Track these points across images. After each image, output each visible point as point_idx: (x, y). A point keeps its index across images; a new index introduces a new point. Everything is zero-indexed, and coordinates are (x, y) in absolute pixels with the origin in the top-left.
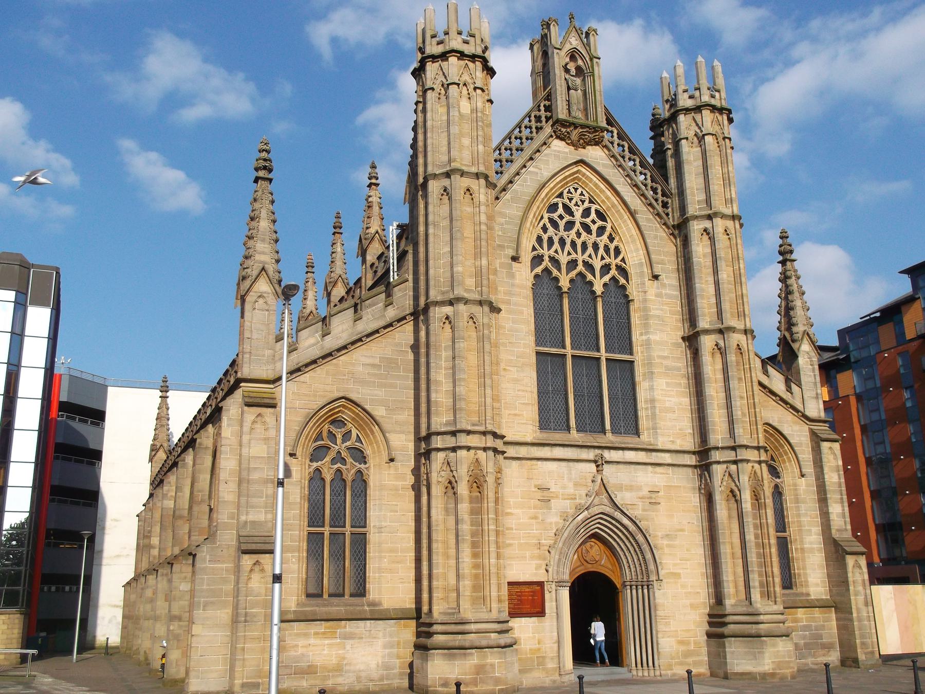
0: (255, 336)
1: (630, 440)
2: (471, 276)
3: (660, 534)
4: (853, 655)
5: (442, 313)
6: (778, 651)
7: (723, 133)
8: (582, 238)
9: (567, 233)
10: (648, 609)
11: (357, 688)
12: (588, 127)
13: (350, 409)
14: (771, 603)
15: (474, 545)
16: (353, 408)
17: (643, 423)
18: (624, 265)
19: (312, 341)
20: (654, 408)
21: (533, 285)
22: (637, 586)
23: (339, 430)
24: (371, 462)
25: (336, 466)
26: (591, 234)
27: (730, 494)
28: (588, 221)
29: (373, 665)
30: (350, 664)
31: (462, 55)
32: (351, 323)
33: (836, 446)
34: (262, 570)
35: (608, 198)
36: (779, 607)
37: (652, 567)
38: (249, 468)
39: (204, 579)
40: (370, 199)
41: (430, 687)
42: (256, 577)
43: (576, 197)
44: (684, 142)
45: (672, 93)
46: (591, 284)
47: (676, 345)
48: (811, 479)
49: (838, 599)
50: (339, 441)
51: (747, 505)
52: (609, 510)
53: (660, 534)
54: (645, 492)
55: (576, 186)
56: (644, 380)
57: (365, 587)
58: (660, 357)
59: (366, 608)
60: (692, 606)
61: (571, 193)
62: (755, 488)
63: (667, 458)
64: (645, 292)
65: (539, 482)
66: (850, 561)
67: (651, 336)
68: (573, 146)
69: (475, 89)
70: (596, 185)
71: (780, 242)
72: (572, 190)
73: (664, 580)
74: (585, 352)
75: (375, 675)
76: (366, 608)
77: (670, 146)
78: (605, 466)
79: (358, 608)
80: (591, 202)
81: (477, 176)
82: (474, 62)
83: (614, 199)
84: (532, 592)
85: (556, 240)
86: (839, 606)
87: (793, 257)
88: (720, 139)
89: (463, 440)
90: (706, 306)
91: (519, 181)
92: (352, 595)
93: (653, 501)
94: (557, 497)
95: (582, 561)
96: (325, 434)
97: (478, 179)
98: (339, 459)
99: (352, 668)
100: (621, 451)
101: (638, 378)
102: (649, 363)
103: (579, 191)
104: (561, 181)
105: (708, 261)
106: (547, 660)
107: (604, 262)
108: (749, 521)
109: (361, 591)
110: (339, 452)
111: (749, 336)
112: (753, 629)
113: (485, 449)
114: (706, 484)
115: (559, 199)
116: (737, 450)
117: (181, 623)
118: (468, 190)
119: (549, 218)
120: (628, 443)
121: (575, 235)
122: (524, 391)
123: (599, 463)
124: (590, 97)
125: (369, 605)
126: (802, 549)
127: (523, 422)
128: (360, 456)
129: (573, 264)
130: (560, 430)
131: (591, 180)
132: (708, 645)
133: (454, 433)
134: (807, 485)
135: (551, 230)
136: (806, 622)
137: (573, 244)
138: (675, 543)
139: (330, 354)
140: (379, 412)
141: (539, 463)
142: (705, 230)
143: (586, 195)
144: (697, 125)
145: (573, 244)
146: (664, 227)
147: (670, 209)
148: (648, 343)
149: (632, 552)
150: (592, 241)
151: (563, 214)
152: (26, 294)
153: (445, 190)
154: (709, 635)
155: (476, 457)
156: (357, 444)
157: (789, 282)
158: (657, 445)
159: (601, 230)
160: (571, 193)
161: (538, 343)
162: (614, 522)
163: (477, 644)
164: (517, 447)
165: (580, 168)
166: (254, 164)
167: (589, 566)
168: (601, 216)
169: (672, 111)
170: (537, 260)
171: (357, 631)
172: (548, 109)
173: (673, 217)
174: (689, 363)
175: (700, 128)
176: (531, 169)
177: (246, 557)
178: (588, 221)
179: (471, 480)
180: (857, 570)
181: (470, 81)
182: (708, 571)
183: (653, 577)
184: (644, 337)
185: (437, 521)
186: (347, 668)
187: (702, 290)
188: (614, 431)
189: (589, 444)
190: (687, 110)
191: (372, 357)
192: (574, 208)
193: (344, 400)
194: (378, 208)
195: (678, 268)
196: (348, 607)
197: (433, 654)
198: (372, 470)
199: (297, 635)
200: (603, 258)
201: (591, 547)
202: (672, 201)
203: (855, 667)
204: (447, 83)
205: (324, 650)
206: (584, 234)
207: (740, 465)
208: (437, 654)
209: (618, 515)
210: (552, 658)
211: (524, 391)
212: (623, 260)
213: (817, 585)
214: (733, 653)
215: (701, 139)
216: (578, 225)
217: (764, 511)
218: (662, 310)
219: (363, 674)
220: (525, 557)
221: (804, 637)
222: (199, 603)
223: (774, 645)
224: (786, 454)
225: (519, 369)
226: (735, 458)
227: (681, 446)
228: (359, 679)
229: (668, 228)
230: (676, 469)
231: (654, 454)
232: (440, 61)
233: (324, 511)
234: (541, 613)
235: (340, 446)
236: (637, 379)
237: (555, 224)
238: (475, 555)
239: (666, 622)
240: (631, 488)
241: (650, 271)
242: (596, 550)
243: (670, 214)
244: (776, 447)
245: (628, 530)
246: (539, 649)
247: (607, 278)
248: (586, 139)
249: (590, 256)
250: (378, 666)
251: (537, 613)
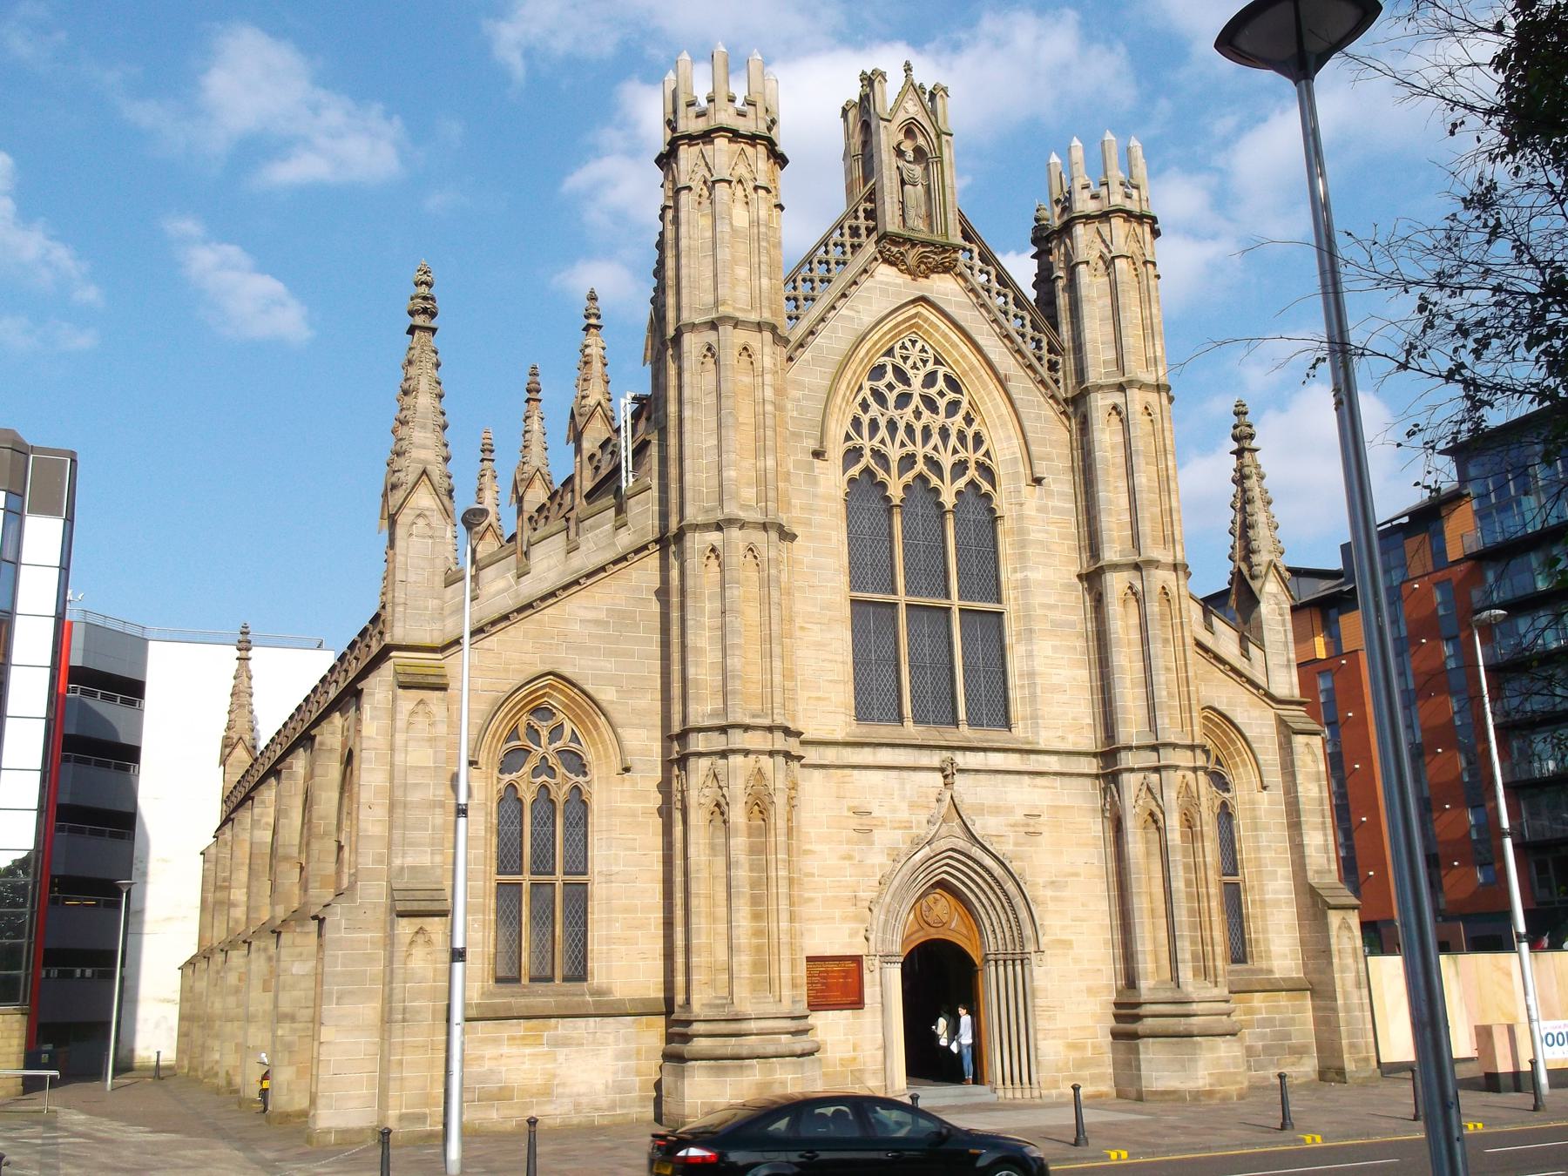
0: (412, 578)
1: (997, 736)
2: (749, 485)
3: (1041, 881)
4: (1336, 1064)
5: (704, 542)
6: (1219, 1058)
7: (1144, 254)
8: (924, 420)
9: (899, 411)
10: (1024, 995)
11: (575, 1121)
12: (933, 245)
13: (561, 691)
14: (1209, 985)
15: (755, 901)
16: (566, 689)
17: (1017, 709)
18: (989, 462)
19: (501, 584)
20: (1033, 685)
21: (847, 494)
22: (1005, 961)
23: (545, 724)
24: (595, 772)
25: (539, 780)
26: (937, 414)
27: (1150, 819)
28: (932, 392)
29: (600, 1087)
30: (564, 1085)
31: (735, 135)
32: (563, 554)
33: (1317, 741)
34: (429, 942)
35: (964, 356)
36: (1223, 991)
37: (1028, 931)
38: (406, 784)
39: (336, 956)
40: (588, 351)
41: (688, 1117)
42: (419, 952)
43: (914, 354)
44: (1082, 268)
45: (1066, 189)
46: (936, 491)
47: (1069, 587)
48: (1277, 793)
49: (1315, 977)
50: (544, 740)
51: (1175, 835)
52: (962, 844)
53: (1041, 881)
54: (1019, 817)
55: (914, 337)
56: (1018, 642)
57: (585, 966)
58: (1043, 606)
59: (589, 998)
60: (1090, 990)
61: (906, 349)
62: (1187, 809)
63: (1053, 763)
64: (1021, 505)
65: (855, 803)
66: (1334, 918)
67: (1029, 574)
68: (910, 274)
69: (756, 188)
70: (945, 336)
71: (1235, 420)
72: (908, 344)
73: (1048, 952)
74: (927, 600)
75: (603, 1101)
76: (589, 998)
77: (1061, 274)
78: (957, 777)
79: (576, 999)
80: (937, 362)
81: (759, 326)
82: (754, 146)
83: (974, 359)
84: (843, 971)
85: (882, 422)
86: (1317, 988)
87: (1254, 444)
88: (1139, 264)
89: (738, 739)
90: (1115, 526)
91: (824, 331)
92: (566, 979)
93: (1031, 830)
94: (882, 826)
95: (922, 923)
96: (522, 730)
97: (761, 331)
98: (544, 768)
99: (567, 1090)
100: (982, 754)
101: (1009, 639)
102: (1026, 616)
103: (919, 346)
104: (890, 330)
105: (1119, 457)
106: (867, 1076)
107: (957, 457)
108: (1177, 858)
109: (578, 972)
110: (544, 757)
111: (1181, 573)
112: (1181, 1025)
113: (771, 754)
114: (1113, 803)
115: (887, 358)
116: (1161, 751)
117: (295, 1025)
118: (745, 349)
119: (871, 389)
120: (993, 741)
121: (912, 416)
122: (831, 661)
123: (947, 773)
124: (935, 194)
125: (592, 994)
126: (1262, 901)
127: (830, 709)
128: (576, 763)
129: (908, 461)
130: (889, 721)
131: (937, 329)
132: (1114, 1051)
133: (723, 730)
134: (1271, 803)
135: (875, 408)
136: (1267, 1013)
137: (910, 429)
138: (1064, 894)
139: (530, 606)
140: (606, 695)
141: (856, 772)
142: (1115, 408)
143: (931, 351)
144: (1104, 241)
145: (910, 429)
146: (1051, 401)
147: (1060, 373)
148: (1024, 585)
149: (998, 908)
150: (938, 424)
151: (894, 381)
152: (22, 496)
153: (709, 349)
154: (1116, 1035)
155: (758, 765)
156: (572, 744)
157: (1248, 484)
158: (1038, 743)
159: (953, 407)
160: (906, 349)
161: (855, 584)
162: (970, 863)
163: (760, 1051)
164: (821, 749)
165: (920, 309)
166: (408, 305)
167: (933, 930)
169: (1065, 218)
170: (853, 455)
171: (575, 1034)
172: (870, 215)
173: (1066, 385)
174: (1088, 616)
175: (1107, 247)
176: (844, 312)
177: (404, 921)
178: (932, 392)
179: (751, 799)
180: (1345, 933)
181: (747, 176)
182: (1115, 937)
183: (1030, 947)
184: (1019, 576)
185: (698, 865)
186: (560, 1090)
187: (1110, 502)
188: (973, 722)
189: (932, 743)
190: (1088, 218)
191: (596, 608)
192: (910, 373)
193: (551, 677)
194: (600, 365)
195: (1073, 467)
196: (561, 998)
197: (693, 1066)
198: (595, 786)
199: (483, 1041)
200: (955, 451)
201: (936, 901)
202: (1064, 360)
203: (1340, 1082)
204: (713, 179)
205: (524, 1063)
206: (926, 413)
207: (1164, 774)
208: (699, 1067)
209: (976, 852)
210: (874, 1073)
211: (831, 661)
212: (987, 453)
213: (1285, 956)
214: (1150, 1061)
215: (1109, 263)
216: (916, 400)
217: (1200, 844)
218: (1047, 532)
219: (584, 1100)
220: (834, 918)
221: (1263, 1036)
222: (331, 993)
223: (1212, 1049)
224: (1239, 754)
225: (823, 627)
226: (1157, 764)
227: (1075, 744)
228: (577, 1107)
229: (1058, 403)
230: (1066, 780)
231: (1033, 757)
232: (701, 145)
233: (521, 848)
234: (857, 1003)
235: (546, 749)
236: (1008, 641)
237: (880, 398)
238: (756, 917)
239: (1050, 1017)
240: (996, 810)
241: (1028, 472)
242: (942, 905)
243: (1061, 381)
244: (1223, 744)
245: (992, 876)
246: (855, 1059)
247: (961, 483)
248: (930, 263)
249: (935, 448)
250: (607, 1087)
251: (852, 1003)
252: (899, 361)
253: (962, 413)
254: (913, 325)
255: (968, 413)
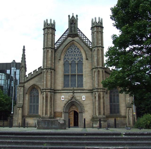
28: (75, 50)
46: (75, 62)
63: (87, 91)
123: (74, 93)
131: (76, 43)
168: (78, 49)
178: (75, 50)
206: (74, 53)
212: (82, 56)
252: (72, 48)
253: (79, 52)
254: (73, 44)
255: (80, 52)
